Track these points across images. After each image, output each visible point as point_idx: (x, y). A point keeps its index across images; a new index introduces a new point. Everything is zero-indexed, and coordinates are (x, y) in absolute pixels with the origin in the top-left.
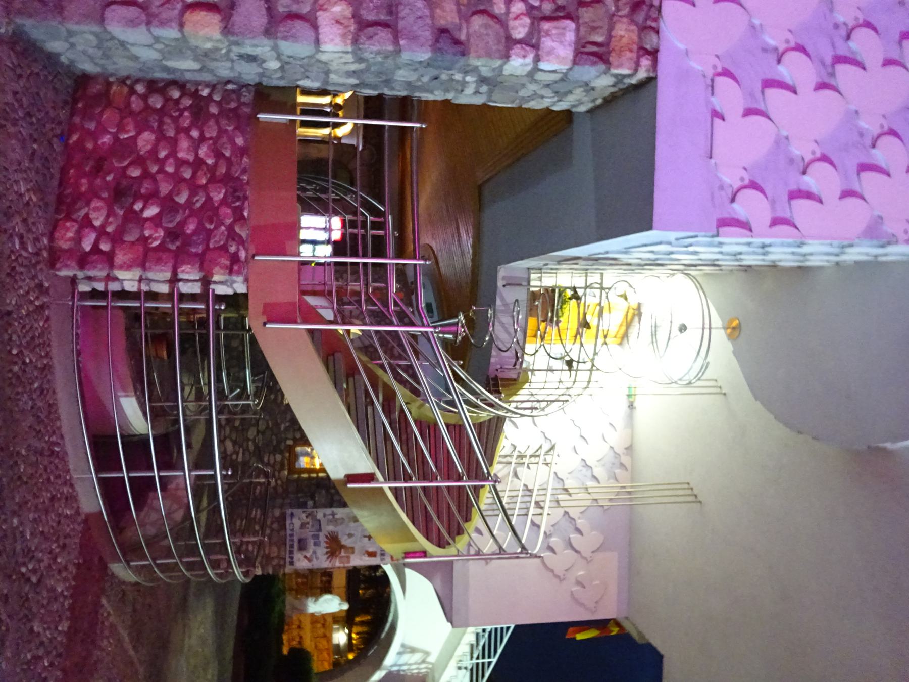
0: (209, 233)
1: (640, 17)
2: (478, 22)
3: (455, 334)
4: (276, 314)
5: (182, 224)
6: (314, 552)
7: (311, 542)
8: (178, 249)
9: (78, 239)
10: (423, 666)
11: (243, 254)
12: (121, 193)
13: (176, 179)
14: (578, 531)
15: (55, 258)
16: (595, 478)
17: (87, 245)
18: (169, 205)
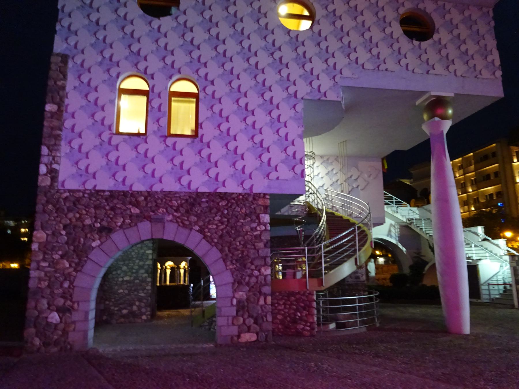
0: (304, 300)
1: (257, 198)
2: (263, 238)
3: (303, 231)
4: (321, 283)
5: (301, 307)
6: (360, 273)
7: (357, 275)
8: (308, 307)
9: (308, 331)
10: (396, 227)
11: (308, 292)
12: (295, 321)
13: (290, 308)
14: (351, 177)
15: (312, 335)
16: (332, 170)
17: (308, 328)
18: (297, 310)
